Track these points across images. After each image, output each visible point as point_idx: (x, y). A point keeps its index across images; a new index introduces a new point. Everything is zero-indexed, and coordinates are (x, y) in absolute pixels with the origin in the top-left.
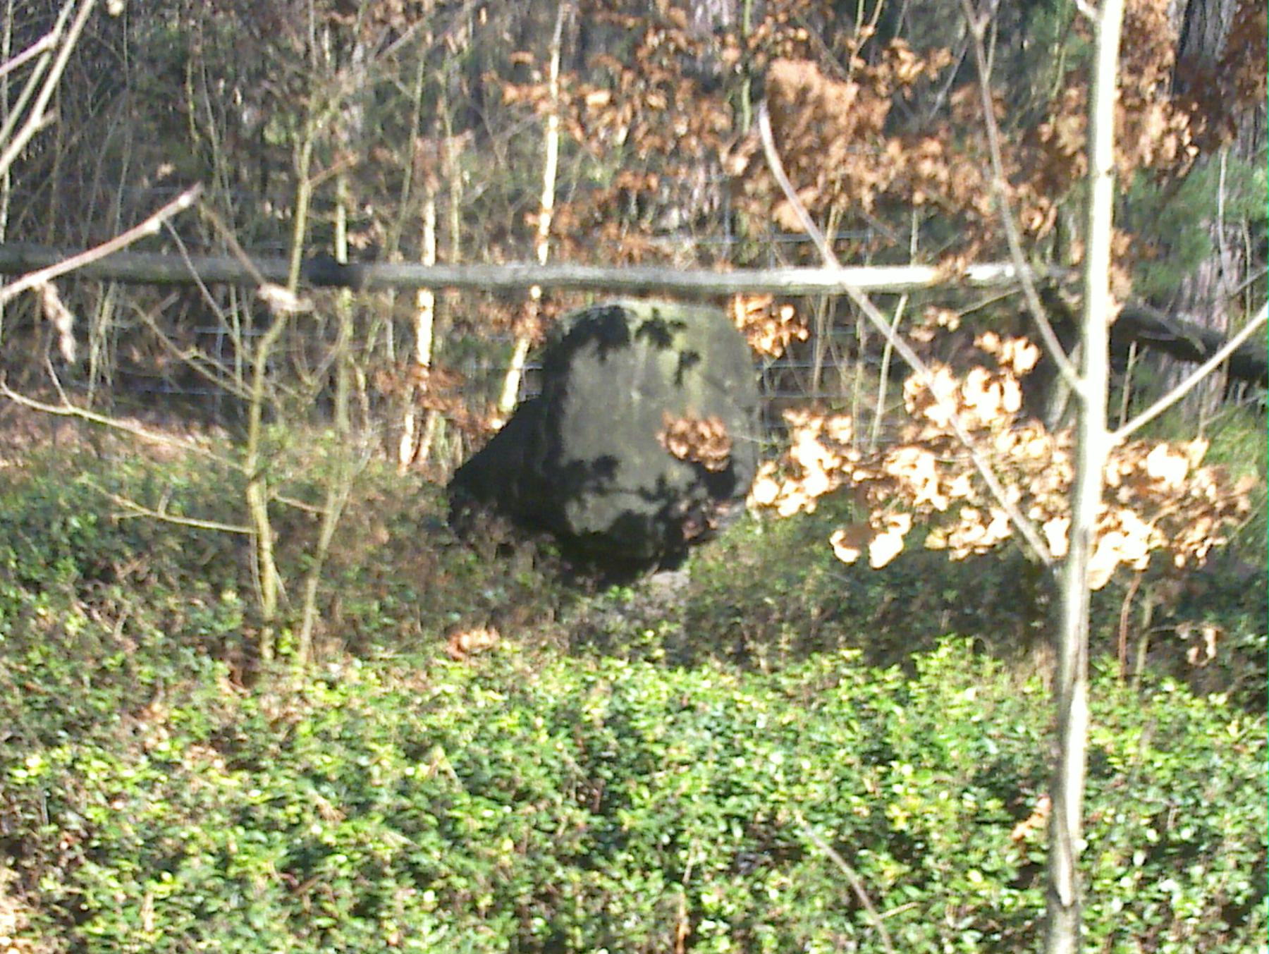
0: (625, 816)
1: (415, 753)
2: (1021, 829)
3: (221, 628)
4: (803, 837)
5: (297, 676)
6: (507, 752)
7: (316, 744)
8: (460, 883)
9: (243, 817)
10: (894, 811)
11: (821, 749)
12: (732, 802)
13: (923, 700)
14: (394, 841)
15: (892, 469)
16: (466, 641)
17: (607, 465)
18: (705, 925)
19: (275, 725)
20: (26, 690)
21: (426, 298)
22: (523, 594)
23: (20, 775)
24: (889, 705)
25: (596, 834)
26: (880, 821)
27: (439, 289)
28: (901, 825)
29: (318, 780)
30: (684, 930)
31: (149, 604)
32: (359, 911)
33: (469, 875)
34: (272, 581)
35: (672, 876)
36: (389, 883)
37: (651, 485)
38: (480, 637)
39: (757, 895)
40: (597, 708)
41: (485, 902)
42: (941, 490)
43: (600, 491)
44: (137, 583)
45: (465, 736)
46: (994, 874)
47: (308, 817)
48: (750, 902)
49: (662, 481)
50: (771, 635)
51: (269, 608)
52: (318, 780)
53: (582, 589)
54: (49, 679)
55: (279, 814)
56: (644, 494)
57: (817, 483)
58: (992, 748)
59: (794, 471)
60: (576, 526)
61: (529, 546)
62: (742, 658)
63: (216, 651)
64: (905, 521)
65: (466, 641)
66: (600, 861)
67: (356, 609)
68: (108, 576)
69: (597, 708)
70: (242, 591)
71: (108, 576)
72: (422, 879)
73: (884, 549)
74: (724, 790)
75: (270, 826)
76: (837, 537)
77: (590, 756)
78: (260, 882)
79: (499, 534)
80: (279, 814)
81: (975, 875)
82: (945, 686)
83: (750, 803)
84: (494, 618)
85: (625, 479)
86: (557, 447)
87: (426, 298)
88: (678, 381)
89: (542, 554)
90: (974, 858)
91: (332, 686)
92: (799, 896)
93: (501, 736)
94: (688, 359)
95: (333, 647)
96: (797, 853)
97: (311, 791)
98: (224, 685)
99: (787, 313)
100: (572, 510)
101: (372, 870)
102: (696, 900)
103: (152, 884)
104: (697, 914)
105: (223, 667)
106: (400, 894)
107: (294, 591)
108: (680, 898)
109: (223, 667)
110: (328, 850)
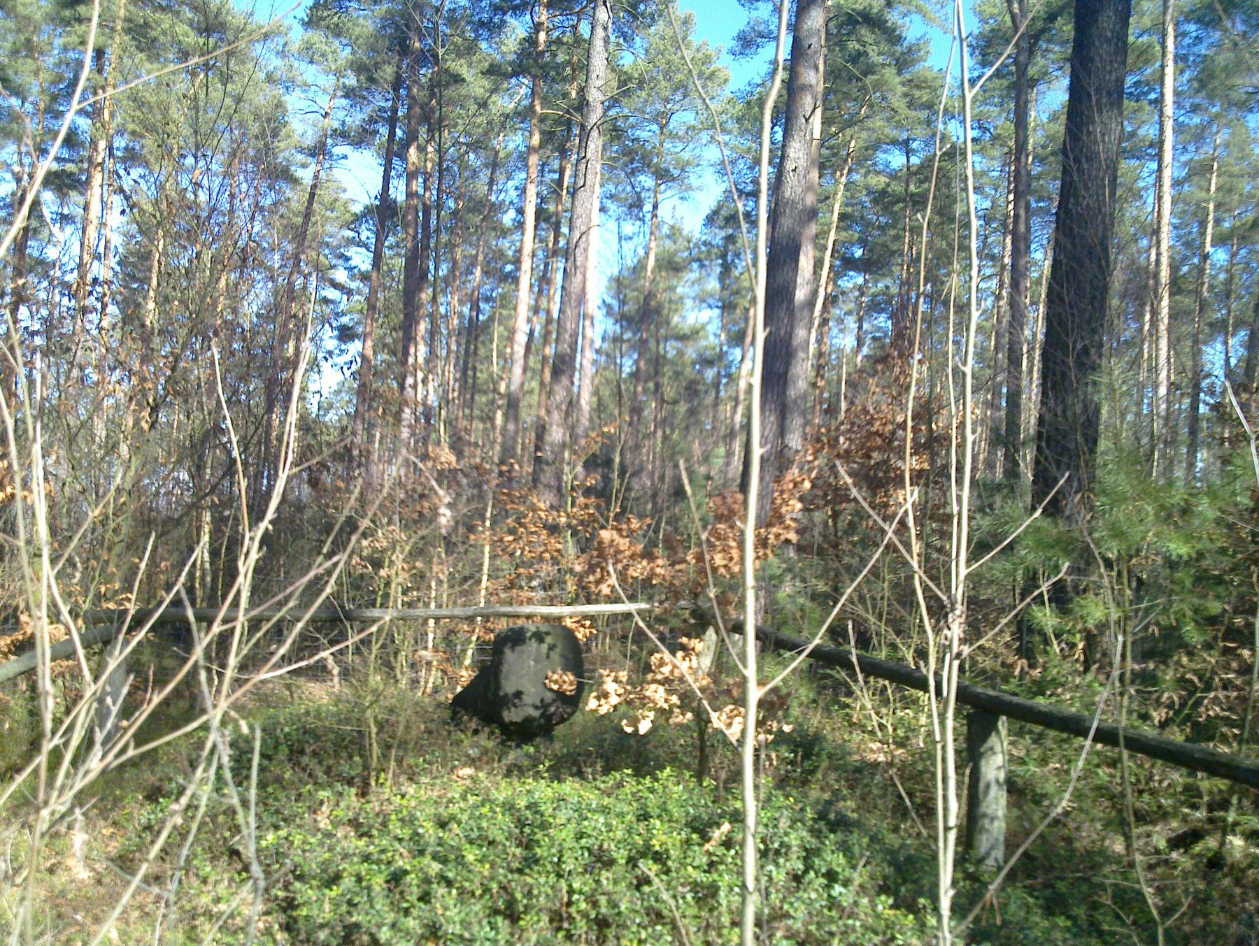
0: (538, 851)
1: (443, 825)
3: (353, 773)
4: (615, 855)
6: (484, 824)
7: (399, 824)
8: (467, 884)
9: (366, 858)
10: (654, 842)
11: (621, 815)
12: (583, 841)
13: (660, 791)
16: (461, 773)
17: (519, 694)
18: (575, 897)
19: (378, 815)
22: (485, 751)
24: (647, 794)
26: (648, 847)
28: (657, 848)
29: (400, 840)
30: (565, 899)
32: (420, 899)
33: (471, 881)
34: (376, 751)
35: (559, 876)
36: (435, 886)
38: (468, 771)
39: (597, 882)
40: (522, 803)
41: (478, 892)
42: (666, 701)
43: (515, 706)
45: (465, 817)
47: (397, 857)
48: (594, 886)
49: (542, 701)
50: (593, 765)
51: (374, 764)
52: (400, 840)
53: (510, 747)
55: (383, 857)
56: (536, 708)
60: (507, 719)
61: (487, 730)
62: (580, 774)
64: (652, 715)
65: (461, 773)
66: (527, 871)
67: (412, 761)
69: (522, 803)
70: (361, 756)
72: (449, 883)
73: (644, 727)
74: (580, 836)
75: (379, 862)
77: (521, 823)
78: (377, 888)
80: (383, 857)
82: (670, 784)
84: (472, 762)
85: (527, 699)
86: (498, 687)
88: (548, 656)
89: (492, 733)
91: (403, 796)
92: (616, 882)
93: (481, 817)
94: (551, 648)
95: (403, 779)
97: (397, 845)
99: (588, 623)
101: (427, 881)
102: (570, 886)
103: (327, 891)
104: (571, 892)
106: (441, 890)
107: (385, 756)
108: (563, 884)
110: (406, 872)
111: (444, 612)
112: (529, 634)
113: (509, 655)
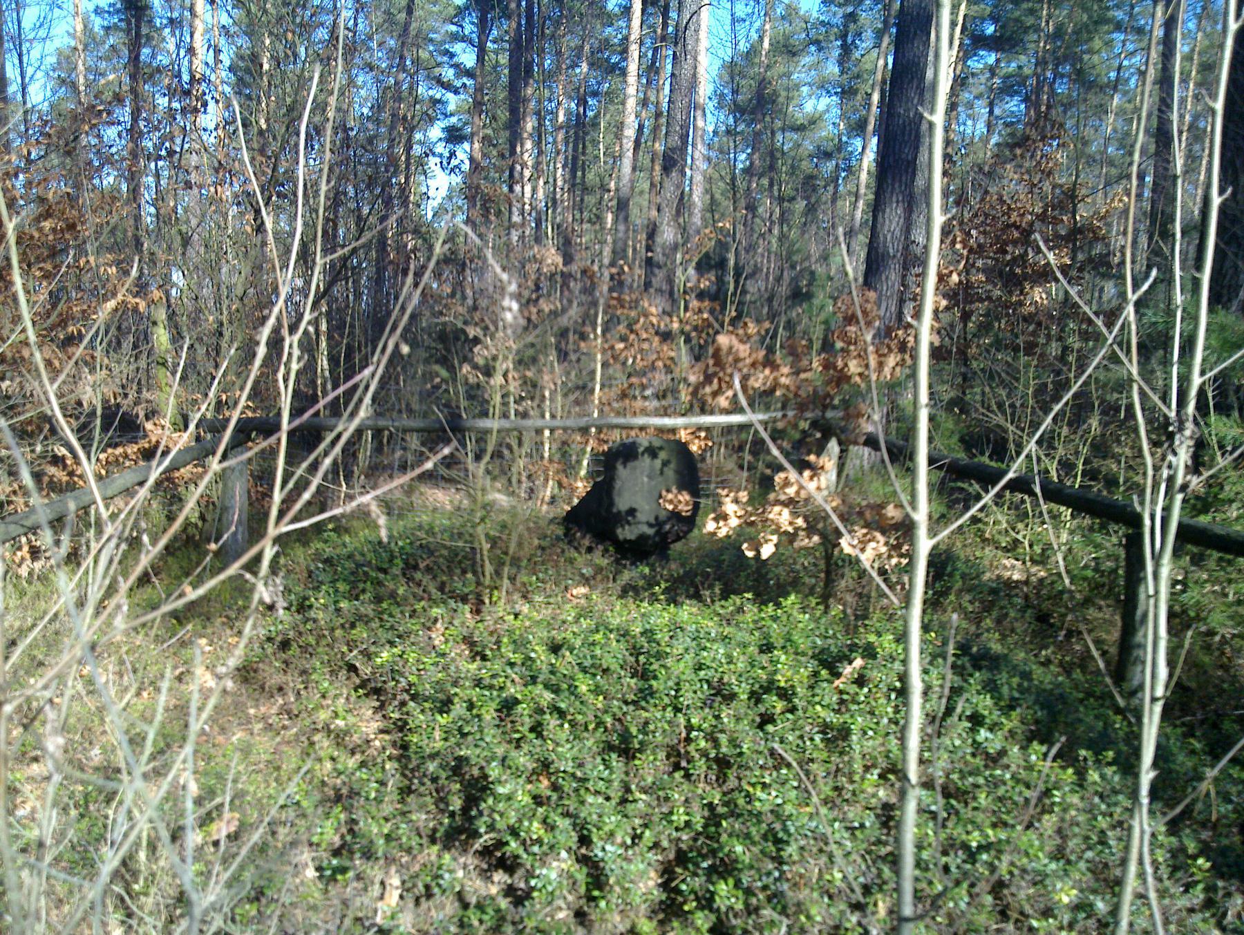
0: (654, 683)
1: (555, 649)
2: (837, 683)
3: (466, 590)
4: (736, 689)
5: (501, 609)
6: (598, 652)
7: (511, 647)
8: (579, 717)
9: (478, 683)
10: (779, 677)
11: (745, 646)
12: (702, 673)
13: (784, 618)
14: (548, 696)
15: (771, 516)
16: (575, 592)
17: (632, 512)
18: (694, 734)
19: (491, 633)
20: (381, 620)
21: (547, 433)
22: (599, 570)
23: (379, 660)
24: (770, 623)
25: (641, 691)
26: (771, 682)
27: (552, 431)
28: (782, 684)
29: (512, 665)
30: (684, 735)
31: (434, 578)
32: (532, 730)
33: (584, 714)
34: (489, 568)
35: (677, 710)
36: (547, 716)
37: (652, 521)
38: (582, 590)
39: (717, 717)
40: (637, 629)
41: (591, 727)
42: (791, 523)
43: (629, 523)
44: (428, 569)
45: (578, 643)
46: (828, 706)
47: (509, 684)
48: (714, 722)
49: (657, 518)
50: (711, 587)
51: (487, 581)
52: (512, 665)
53: (625, 566)
54: (391, 615)
55: (495, 682)
56: (650, 525)
57: (734, 522)
58: (819, 642)
59: (725, 517)
60: (621, 537)
61: (601, 547)
62: (697, 596)
63: (464, 599)
64: (775, 538)
65: (575, 592)
66: (643, 703)
67: (525, 579)
68: (416, 567)
69: (637, 629)
70: (475, 573)
71: (416, 567)
72: (562, 714)
73: (767, 551)
74: (699, 667)
75: (491, 687)
76: (745, 546)
77: (636, 651)
78: (487, 717)
79: (586, 542)
80: (495, 682)
81: (818, 708)
82: (795, 613)
83: (711, 673)
84: (586, 581)
85: (641, 517)
86: (611, 503)
87: (547, 433)
88: (662, 473)
89: (606, 551)
90: (817, 699)
91: (516, 616)
92: (738, 719)
93: (593, 644)
95: (516, 596)
96: (732, 696)
97: (509, 671)
98: (469, 616)
99: (703, 434)
100: (619, 531)
101: (540, 711)
102: (689, 721)
103: (438, 717)
104: (690, 728)
105: (467, 608)
106: (551, 721)
107: (498, 573)
108: (681, 720)
109: (467, 608)
110: (517, 702)
111: (557, 423)
112: (641, 450)
113: (622, 472)
